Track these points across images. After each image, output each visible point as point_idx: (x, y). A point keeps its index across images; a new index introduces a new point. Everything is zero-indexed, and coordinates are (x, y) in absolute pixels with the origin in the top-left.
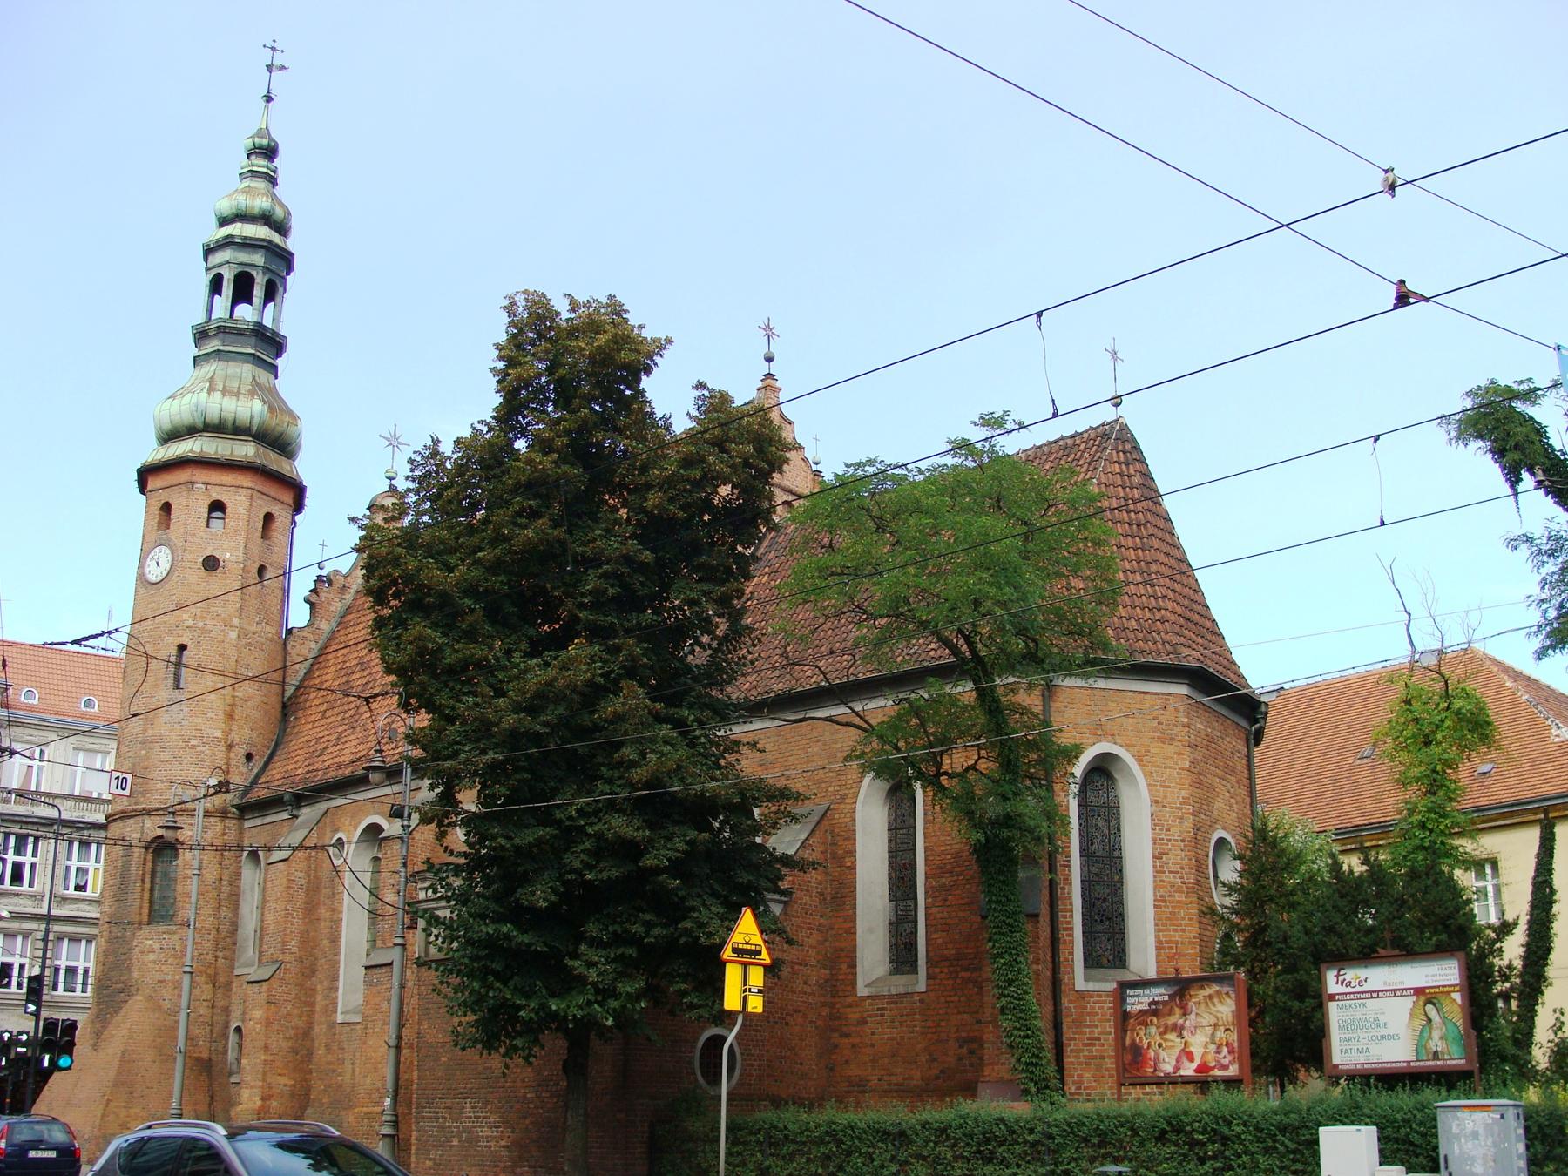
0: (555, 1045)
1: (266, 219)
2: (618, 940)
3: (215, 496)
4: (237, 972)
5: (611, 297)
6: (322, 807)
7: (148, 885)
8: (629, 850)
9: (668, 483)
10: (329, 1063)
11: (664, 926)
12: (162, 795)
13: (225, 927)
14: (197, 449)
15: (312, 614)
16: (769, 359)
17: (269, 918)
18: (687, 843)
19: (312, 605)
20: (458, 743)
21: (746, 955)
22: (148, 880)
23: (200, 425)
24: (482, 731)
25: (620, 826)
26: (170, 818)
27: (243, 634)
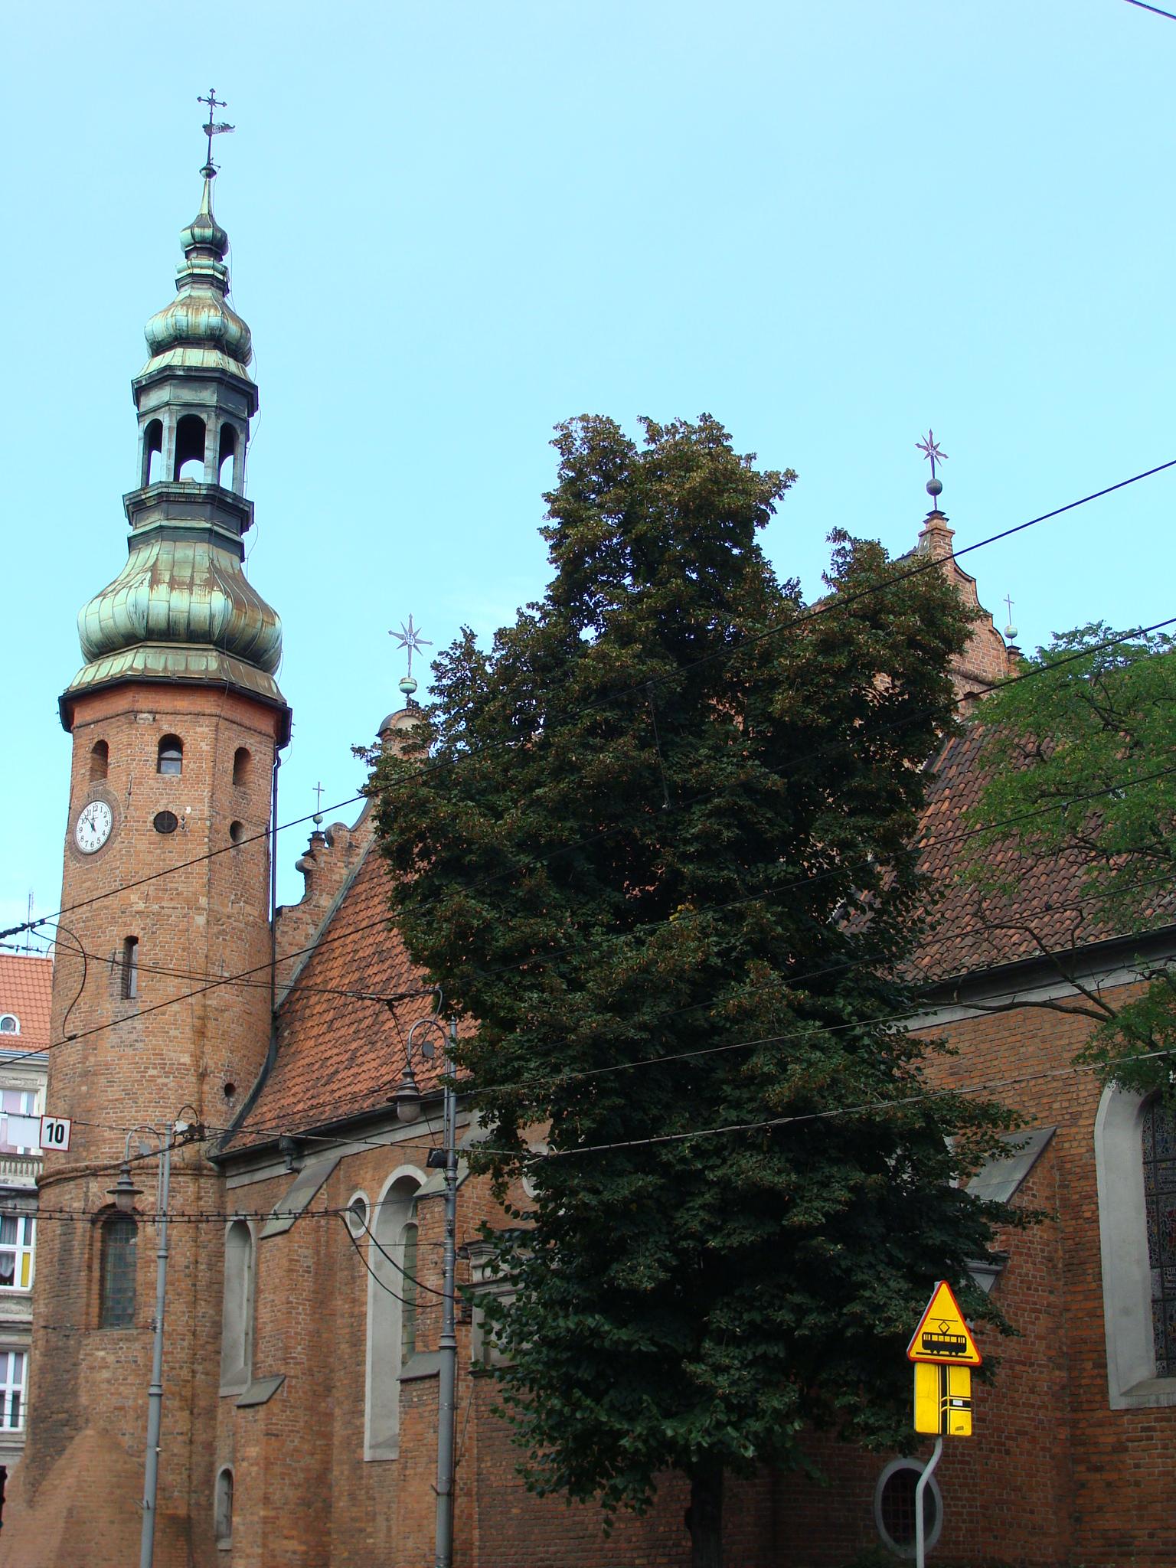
0: (673, 1488)
1: (215, 339)
2: (757, 1333)
3: (167, 729)
4: (223, 1392)
5: (705, 418)
6: (332, 1156)
7: (96, 1274)
8: (768, 1203)
9: (801, 677)
10: (353, 1519)
11: (824, 1311)
12: (112, 1148)
13: (204, 1330)
14: (139, 665)
15: (309, 886)
16: (935, 490)
17: (265, 1314)
18: (851, 1189)
19: (308, 874)
20: (520, 1058)
21: (944, 1350)
22: (96, 1266)
23: (141, 632)
24: (552, 1041)
25: (753, 1168)
26: (124, 1178)
27: (214, 918)
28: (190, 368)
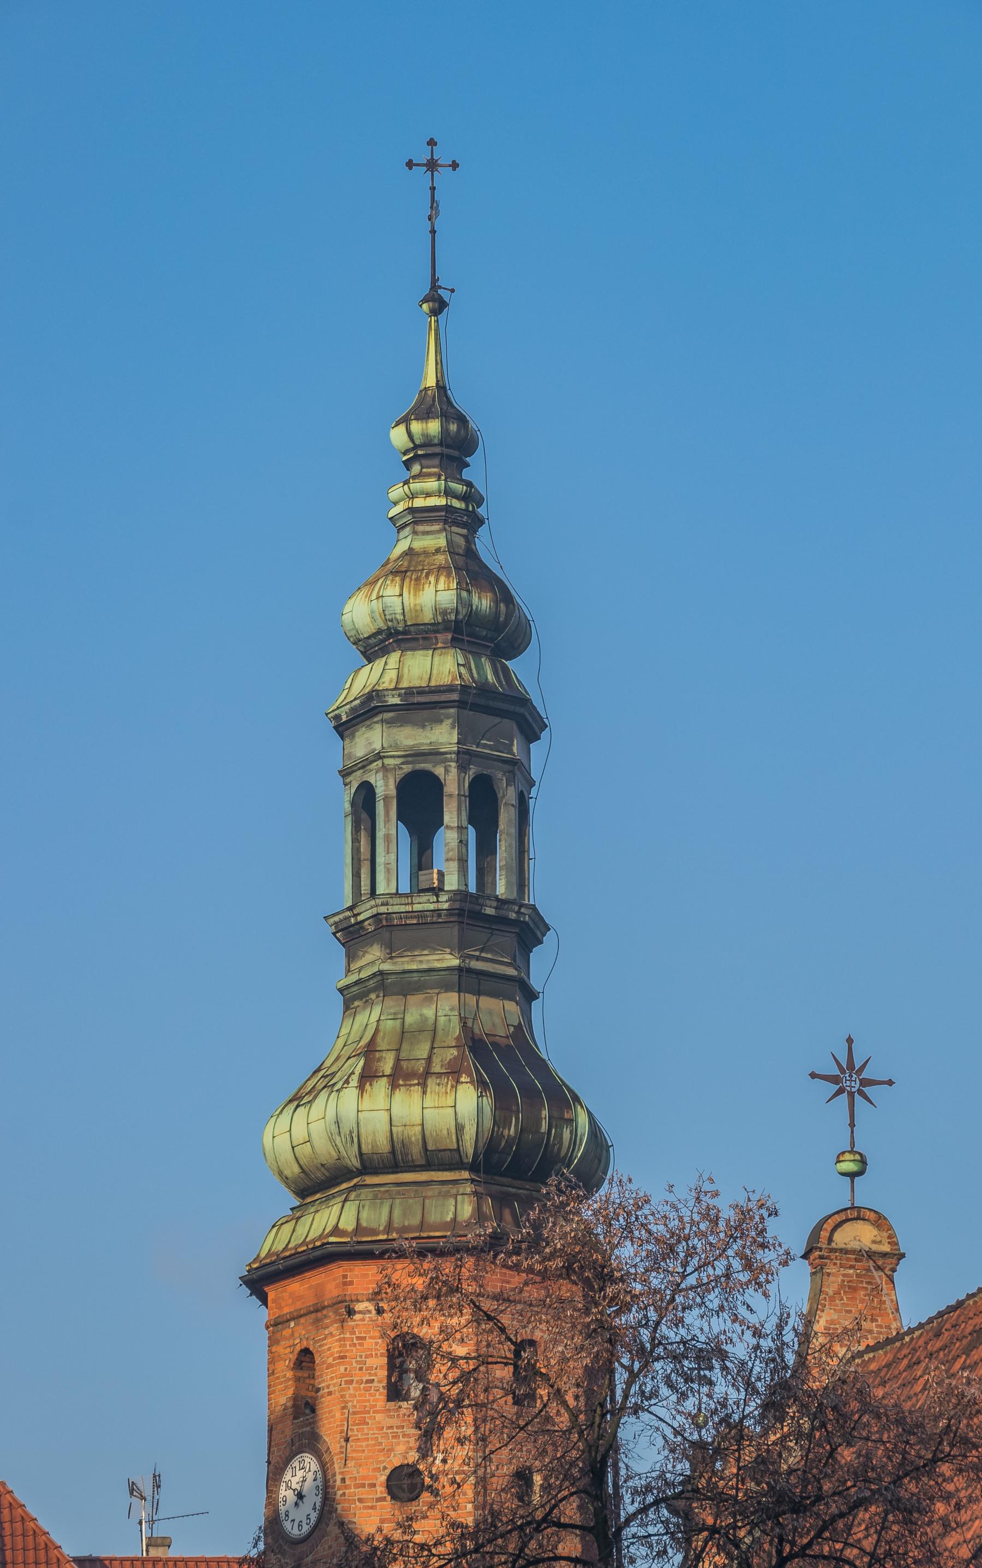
28: (410, 691)
